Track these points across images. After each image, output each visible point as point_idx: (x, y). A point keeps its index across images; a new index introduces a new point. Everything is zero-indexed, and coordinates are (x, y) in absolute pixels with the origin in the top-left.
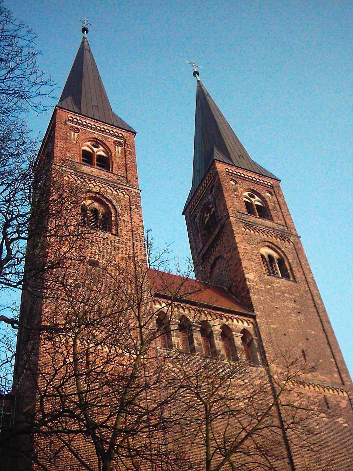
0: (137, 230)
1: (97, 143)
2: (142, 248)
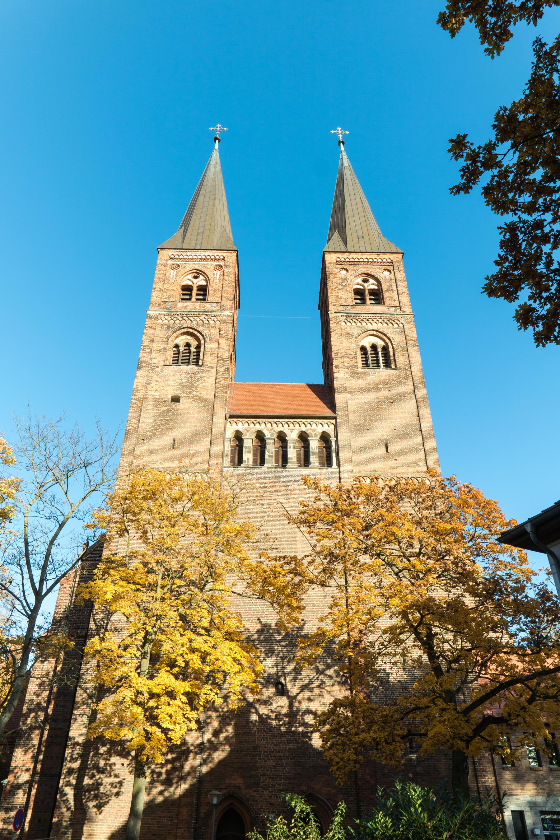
1: (197, 273)
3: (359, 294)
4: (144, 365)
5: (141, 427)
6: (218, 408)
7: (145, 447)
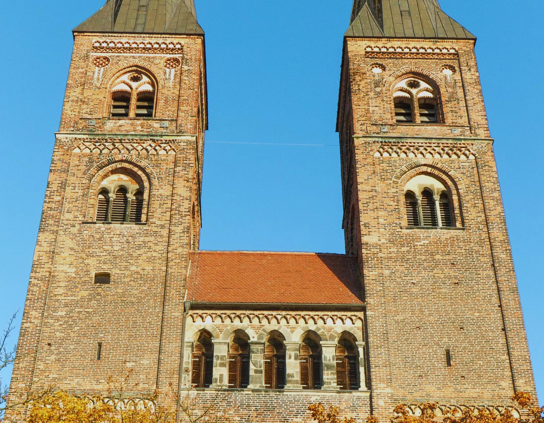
0: (180, 206)
1: (138, 73)
2: (182, 235)
3: (404, 106)
4: (51, 222)
5: (46, 324)
6: (172, 293)
7: (53, 357)
